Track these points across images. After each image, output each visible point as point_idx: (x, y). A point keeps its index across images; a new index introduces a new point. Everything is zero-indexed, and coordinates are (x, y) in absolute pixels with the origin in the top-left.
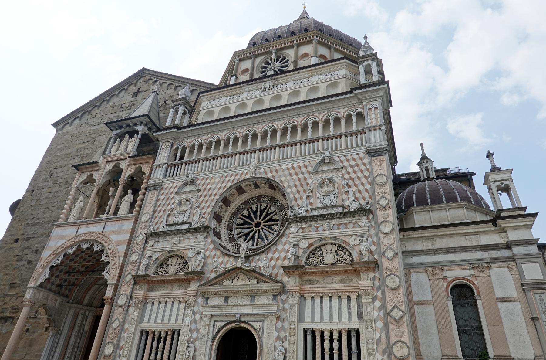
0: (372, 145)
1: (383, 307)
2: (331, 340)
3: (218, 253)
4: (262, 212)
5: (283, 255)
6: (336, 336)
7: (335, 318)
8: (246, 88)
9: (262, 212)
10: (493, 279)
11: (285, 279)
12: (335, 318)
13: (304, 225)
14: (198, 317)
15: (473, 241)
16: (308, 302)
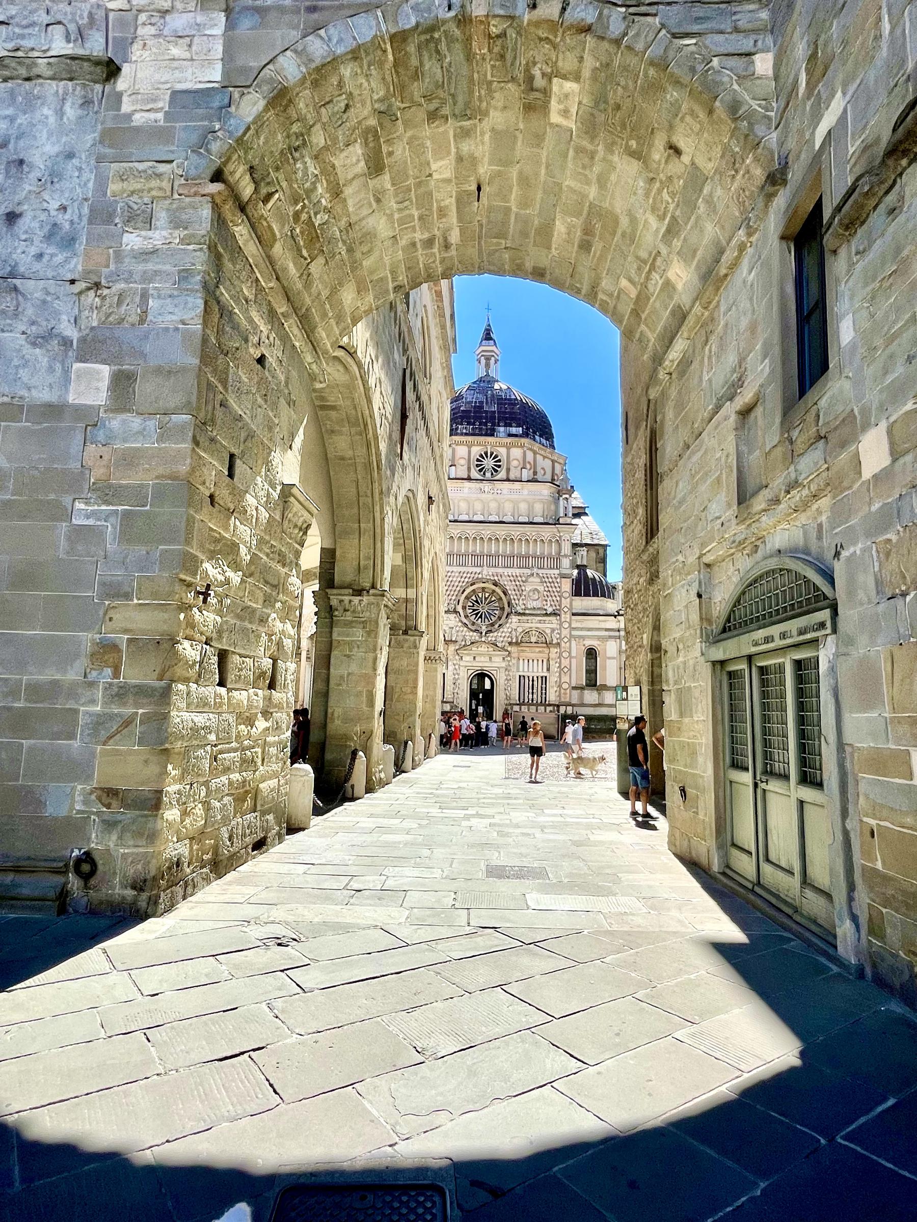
0: (564, 571)
1: (559, 667)
2: (533, 681)
3: (466, 629)
4: (486, 599)
5: (508, 635)
6: (535, 679)
7: (535, 670)
8: (467, 484)
9: (486, 599)
10: (608, 647)
11: (509, 649)
12: (535, 670)
13: (520, 618)
14: (457, 667)
15: (603, 625)
16: (521, 661)
